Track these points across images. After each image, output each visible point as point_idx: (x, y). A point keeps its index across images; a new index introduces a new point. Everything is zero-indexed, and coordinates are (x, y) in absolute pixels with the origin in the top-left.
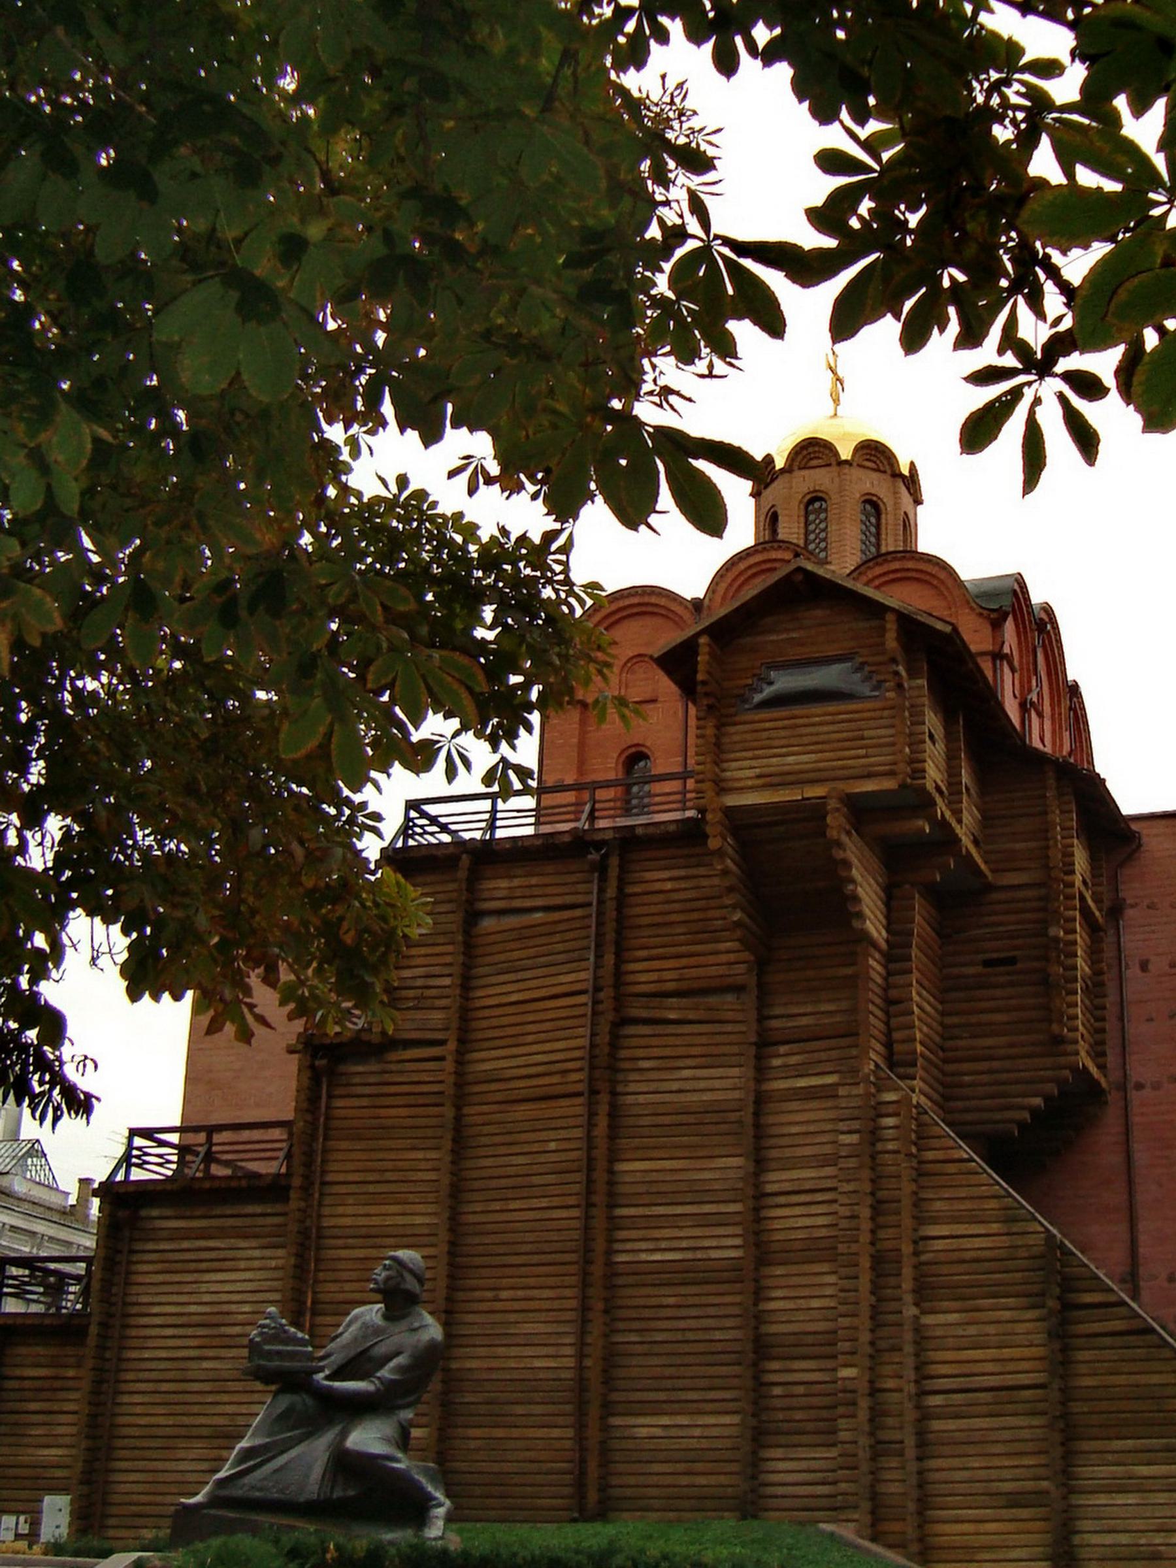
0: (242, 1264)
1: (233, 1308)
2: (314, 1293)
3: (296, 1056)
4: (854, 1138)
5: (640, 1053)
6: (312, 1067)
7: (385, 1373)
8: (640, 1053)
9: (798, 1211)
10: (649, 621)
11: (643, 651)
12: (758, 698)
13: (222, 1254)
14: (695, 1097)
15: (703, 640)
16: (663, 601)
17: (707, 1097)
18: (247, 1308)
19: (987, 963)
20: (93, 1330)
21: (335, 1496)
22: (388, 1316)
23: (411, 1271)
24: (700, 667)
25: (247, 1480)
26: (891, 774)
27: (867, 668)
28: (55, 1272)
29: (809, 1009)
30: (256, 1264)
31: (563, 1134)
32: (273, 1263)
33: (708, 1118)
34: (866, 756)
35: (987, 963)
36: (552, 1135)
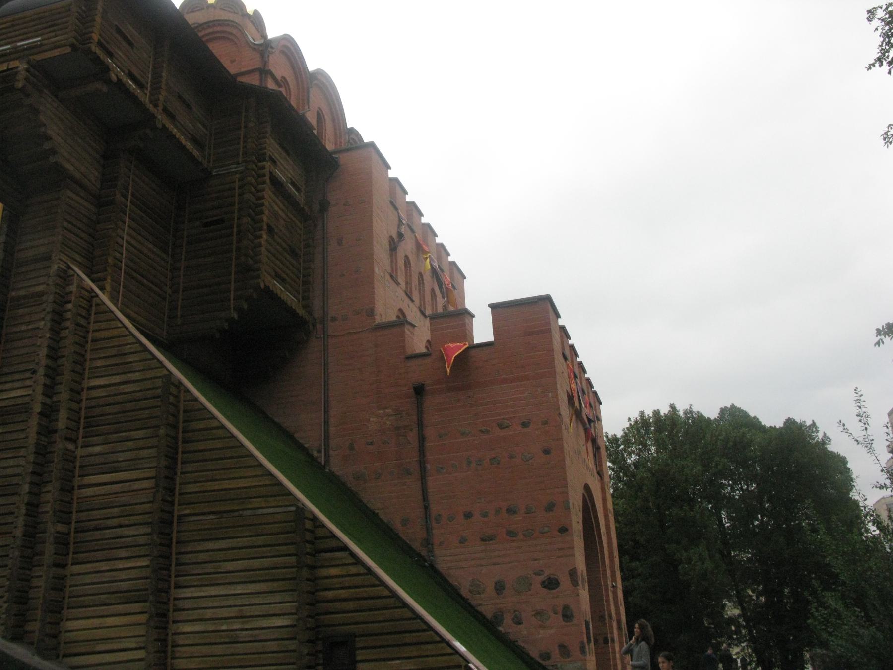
9: (17, 384)
19: (206, 225)
35: (206, 225)
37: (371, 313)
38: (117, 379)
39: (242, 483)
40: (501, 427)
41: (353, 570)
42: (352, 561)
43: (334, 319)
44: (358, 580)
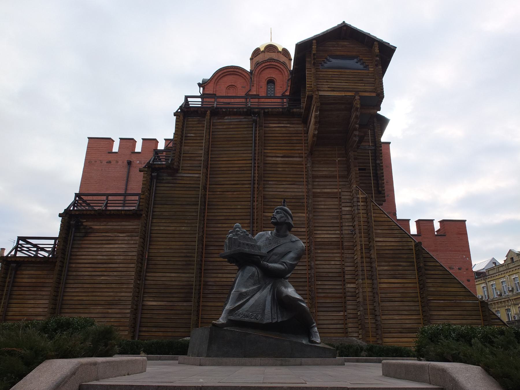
0: (120, 242)
1: (116, 257)
2: (148, 252)
5: (269, 179)
6: (151, 175)
7: (288, 259)
8: (269, 179)
10: (235, 76)
11: (233, 84)
12: (326, 65)
13: (112, 238)
14: (289, 194)
15: (314, 41)
16: (240, 71)
17: (293, 194)
18: (122, 257)
20: (58, 264)
21: (279, 320)
24: (314, 49)
25: (240, 311)
26: (374, 92)
28: (35, 246)
29: (326, 169)
30: (126, 242)
31: (243, 203)
32: (132, 242)
33: (293, 201)
36: (239, 203)
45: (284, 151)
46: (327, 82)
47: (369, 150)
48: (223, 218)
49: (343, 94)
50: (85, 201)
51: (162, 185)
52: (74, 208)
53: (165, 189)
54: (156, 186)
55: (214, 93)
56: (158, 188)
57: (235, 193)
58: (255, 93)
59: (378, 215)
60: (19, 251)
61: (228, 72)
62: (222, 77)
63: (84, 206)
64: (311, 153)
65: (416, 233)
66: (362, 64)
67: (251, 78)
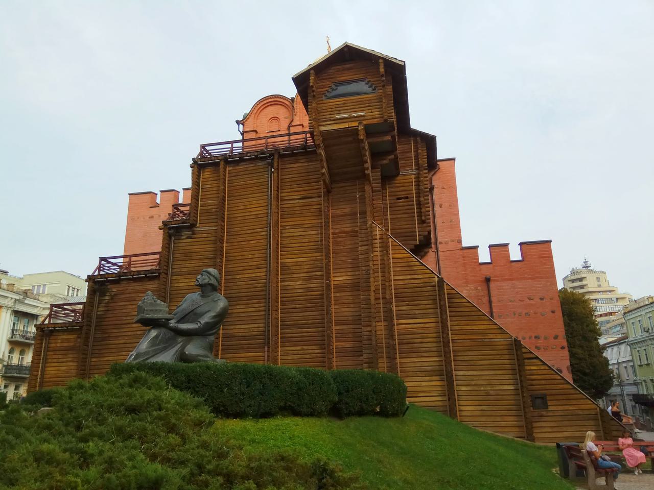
3: (162, 230)
4: (364, 248)
6: (168, 232)
9: (344, 274)
22: (202, 296)
23: (214, 276)
27: (370, 83)
34: (372, 112)
37: (460, 242)
38: (409, 277)
39: (482, 327)
40: (530, 299)
41: (542, 367)
42: (541, 363)
43: (441, 243)
44: (545, 372)
45: (302, 193)
46: (330, 114)
47: (411, 175)
48: (241, 268)
49: (346, 125)
50: (114, 264)
51: (181, 241)
52: (99, 272)
53: (184, 244)
54: (174, 243)
55: (255, 129)
56: (176, 245)
57: (252, 242)
58: (298, 123)
59: (397, 252)
60: (53, 318)
61: (273, 101)
62: (263, 109)
63: (114, 269)
64: (328, 192)
65: (521, 259)
66: (371, 86)
67: (293, 106)
